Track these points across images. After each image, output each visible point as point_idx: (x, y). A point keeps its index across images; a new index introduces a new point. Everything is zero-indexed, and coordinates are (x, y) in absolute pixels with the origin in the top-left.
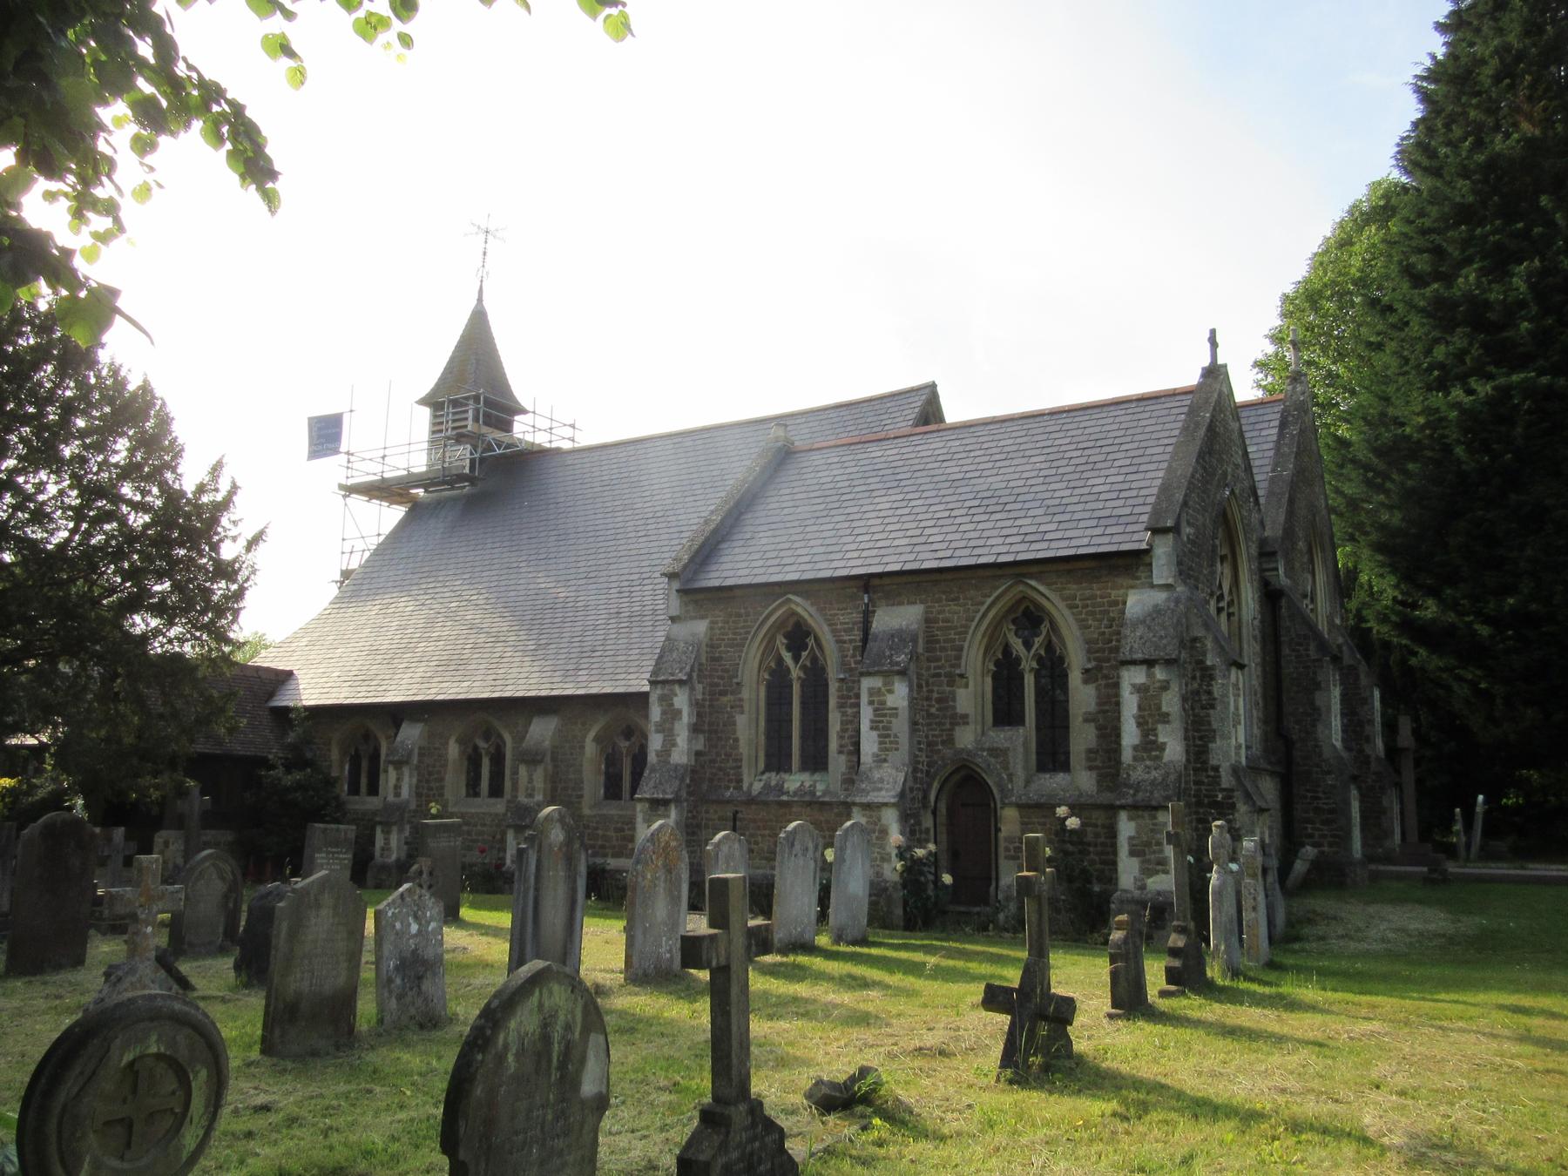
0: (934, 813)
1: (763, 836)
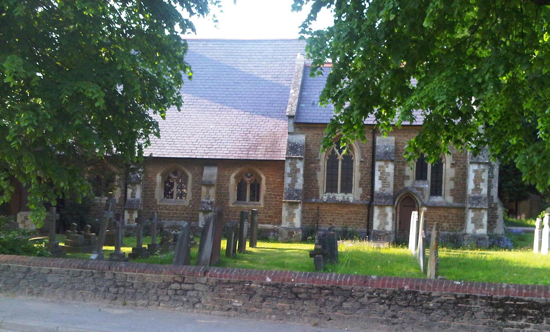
1: (327, 216)
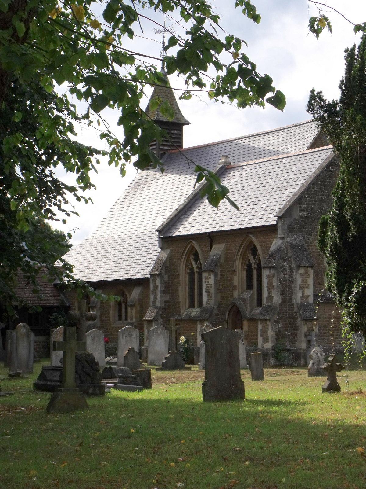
0: (227, 323)
